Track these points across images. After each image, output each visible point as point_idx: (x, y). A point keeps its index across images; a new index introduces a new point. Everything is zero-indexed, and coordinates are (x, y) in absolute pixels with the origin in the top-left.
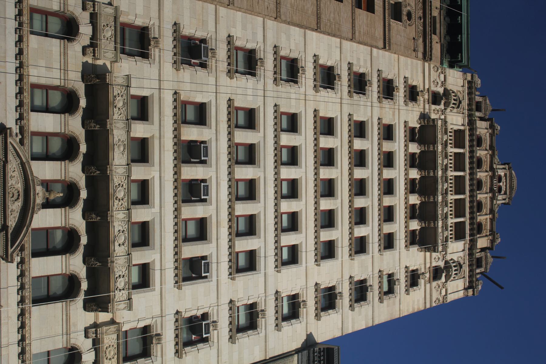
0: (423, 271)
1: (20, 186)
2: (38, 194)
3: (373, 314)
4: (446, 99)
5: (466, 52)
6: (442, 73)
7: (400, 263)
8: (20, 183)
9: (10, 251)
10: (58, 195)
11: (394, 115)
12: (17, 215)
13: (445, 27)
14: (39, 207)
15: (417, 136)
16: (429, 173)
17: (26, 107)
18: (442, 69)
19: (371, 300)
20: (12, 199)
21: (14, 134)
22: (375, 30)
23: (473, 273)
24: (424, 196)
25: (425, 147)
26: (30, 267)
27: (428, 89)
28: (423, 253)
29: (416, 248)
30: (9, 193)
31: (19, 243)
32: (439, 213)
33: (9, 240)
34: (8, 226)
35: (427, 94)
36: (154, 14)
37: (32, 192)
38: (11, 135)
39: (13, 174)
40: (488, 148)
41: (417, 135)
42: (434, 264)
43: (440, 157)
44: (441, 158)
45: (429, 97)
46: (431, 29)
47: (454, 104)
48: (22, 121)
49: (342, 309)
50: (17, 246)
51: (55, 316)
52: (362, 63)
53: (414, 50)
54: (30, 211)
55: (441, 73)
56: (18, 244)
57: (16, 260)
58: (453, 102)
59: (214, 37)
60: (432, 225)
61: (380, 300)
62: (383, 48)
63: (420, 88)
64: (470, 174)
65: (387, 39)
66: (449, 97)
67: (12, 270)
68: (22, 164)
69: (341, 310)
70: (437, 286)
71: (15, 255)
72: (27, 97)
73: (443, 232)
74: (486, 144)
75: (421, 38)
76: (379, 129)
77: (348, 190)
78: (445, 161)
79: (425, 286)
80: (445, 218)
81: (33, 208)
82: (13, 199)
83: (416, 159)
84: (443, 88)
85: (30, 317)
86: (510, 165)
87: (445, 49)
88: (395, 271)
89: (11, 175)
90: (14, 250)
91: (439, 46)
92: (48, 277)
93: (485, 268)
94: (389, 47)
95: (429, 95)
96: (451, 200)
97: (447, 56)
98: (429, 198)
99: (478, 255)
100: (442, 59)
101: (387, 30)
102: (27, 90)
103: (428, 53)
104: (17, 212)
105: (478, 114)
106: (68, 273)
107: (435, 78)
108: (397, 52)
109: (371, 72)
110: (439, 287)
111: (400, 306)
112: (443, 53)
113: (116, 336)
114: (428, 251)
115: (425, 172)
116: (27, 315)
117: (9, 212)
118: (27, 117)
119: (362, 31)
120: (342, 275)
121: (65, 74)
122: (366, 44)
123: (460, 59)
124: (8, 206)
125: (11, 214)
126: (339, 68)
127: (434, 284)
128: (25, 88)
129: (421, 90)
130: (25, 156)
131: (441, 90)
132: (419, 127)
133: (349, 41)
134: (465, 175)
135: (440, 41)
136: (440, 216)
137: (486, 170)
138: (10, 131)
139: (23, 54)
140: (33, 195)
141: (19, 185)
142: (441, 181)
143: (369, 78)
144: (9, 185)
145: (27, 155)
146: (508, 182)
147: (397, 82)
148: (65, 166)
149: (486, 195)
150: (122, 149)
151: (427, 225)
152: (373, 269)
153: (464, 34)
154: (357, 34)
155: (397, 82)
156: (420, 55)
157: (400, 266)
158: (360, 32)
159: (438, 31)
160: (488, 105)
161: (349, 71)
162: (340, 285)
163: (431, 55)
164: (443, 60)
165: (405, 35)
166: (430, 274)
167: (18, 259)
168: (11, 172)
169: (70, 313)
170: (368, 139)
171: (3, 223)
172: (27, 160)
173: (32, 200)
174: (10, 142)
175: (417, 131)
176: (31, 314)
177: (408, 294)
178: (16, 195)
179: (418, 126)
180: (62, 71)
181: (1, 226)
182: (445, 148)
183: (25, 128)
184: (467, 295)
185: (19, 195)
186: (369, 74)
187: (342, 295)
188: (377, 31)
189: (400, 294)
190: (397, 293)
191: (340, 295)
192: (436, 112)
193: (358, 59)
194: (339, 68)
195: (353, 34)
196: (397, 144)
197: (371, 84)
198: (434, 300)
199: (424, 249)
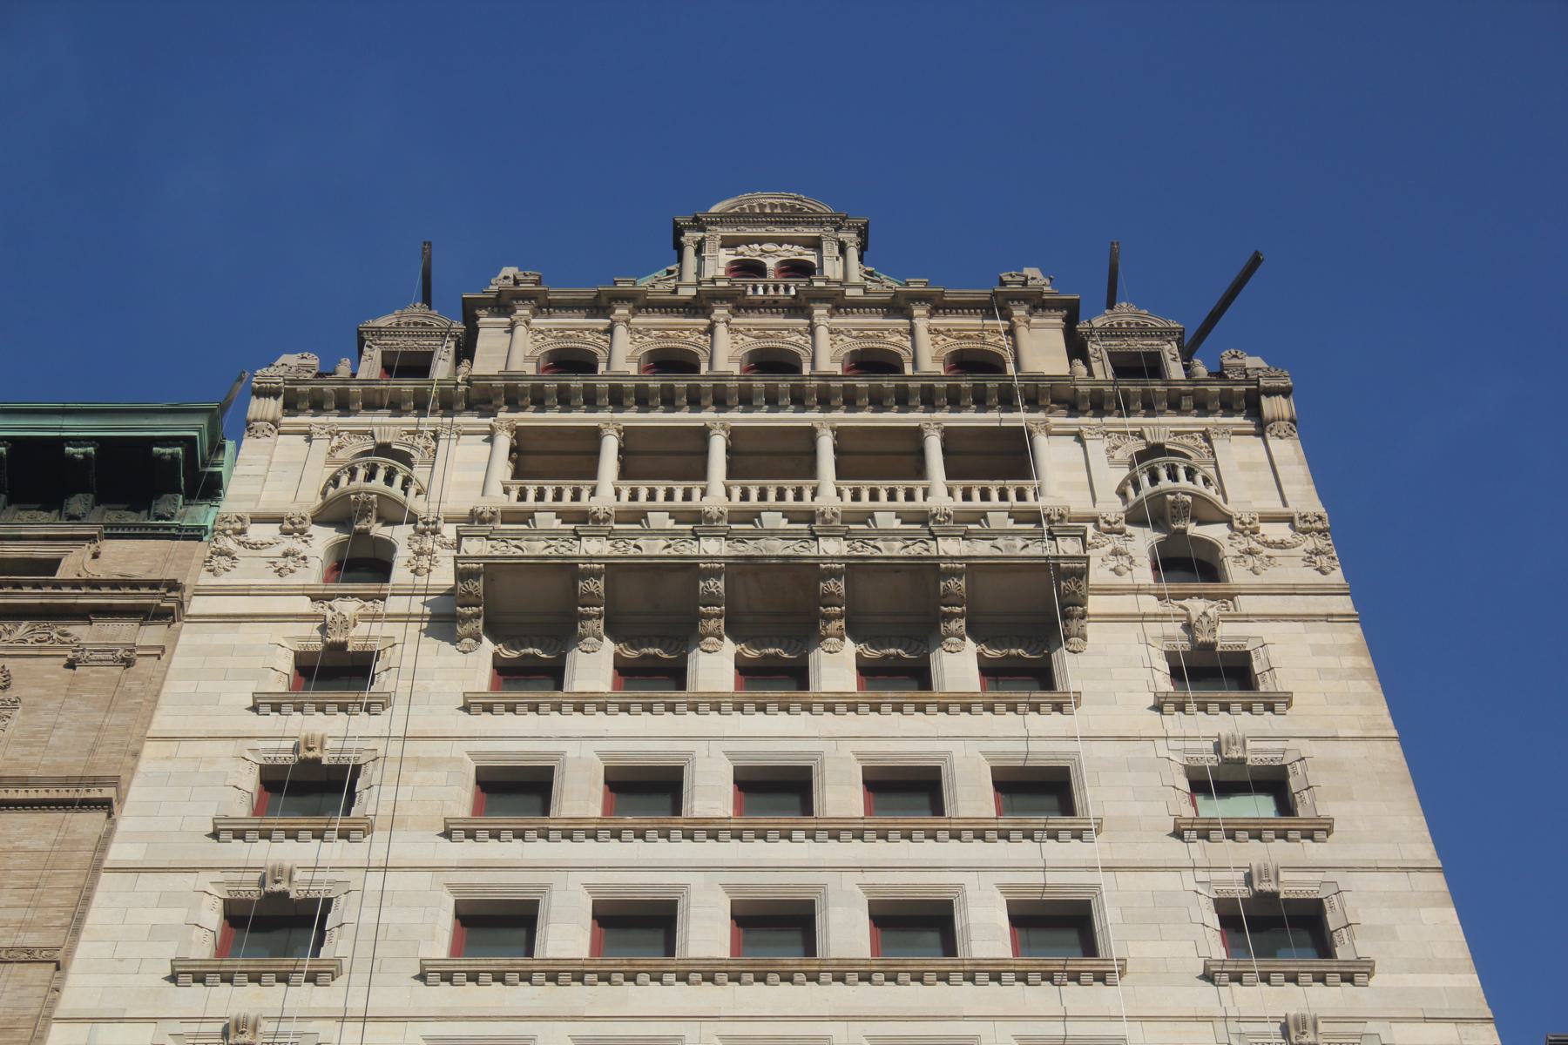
0: (1175, 629)
3: (1388, 869)
4: (364, 514)
5: (146, 422)
6: (242, 532)
7: (1140, 738)
11: (431, 763)
13: (25, 515)
15: (538, 652)
16: (712, 600)
18: (224, 531)
19: (1319, 876)
22: (16, 849)
23: (1186, 394)
24: (822, 623)
25: (589, 617)
27: (314, 598)
28: (1091, 629)
29: (1068, 657)
32: (903, 553)
35: (336, 603)
40: (602, 323)
41: (531, 650)
42: (1144, 574)
43: (636, 546)
44: (641, 542)
45: (353, 596)
46: (27, 584)
47: (389, 480)
49: (1363, 1020)
52: (176, 916)
53: (128, 663)
55: (242, 538)
58: (378, 483)
60: (957, 585)
61: (1318, 835)
62: (109, 815)
63: (309, 639)
64: (721, 404)
65: (63, 794)
66: (356, 503)
69: (1371, 1027)
70: (1250, 559)
73: (990, 536)
74: (582, 331)
75: (70, 629)
76: (495, 835)
77: (786, 986)
78: (660, 520)
79: (1247, 618)
80: (925, 523)
83: (645, 656)
84: (314, 530)
86: (683, 220)
87: (131, 518)
88: (1178, 759)
91: (111, 548)
93: (1160, 337)
94: (105, 785)
95: (344, 596)
96: (839, 493)
97: (161, 507)
98: (830, 599)
99: (1103, 371)
100: (173, 531)
101: (21, 795)
103: (145, 598)
105: (442, 368)
107: (263, 563)
108: (133, 747)
109: (223, 869)
110: (1250, 552)
111: (1346, 738)
112: (147, 527)
114: (1082, 603)
115: (709, 617)
119: (17, 915)
120: (1197, 1019)
122: (85, 898)
123: (179, 450)
126: (194, 1028)
127: (1237, 574)
129: (318, 634)
131: (324, 538)
132: (495, 640)
133: (63, 978)
134: (723, 428)
135: (91, 538)
136: (917, 549)
137: (705, 333)
142: (752, 543)
143: (248, 883)
146: (760, 232)
147: (274, 744)
149: (822, 334)
151: (958, 610)
152: (1166, 869)
153: (61, 429)
154: (31, 939)
155: (274, 744)
156: (152, 634)
157: (1152, 738)
158: (24, 926)
159: (42, 551)
160: (403, 320)
161: (209, 978)
162: (1245, 1027)
163: (154, 585)
164: (180, 528)
165: (52, 705)
166: (1191, 596)
170: (545, 888)
175: (514, 654)
177: (1287, 699)
179: (488, 647)
182: (597, 521)
184: (1292, 420)
186: (231, 883)
187: (1296, 1019)
188: (24, 843)
189: (1286, 738)
190: (1284, 751)
191: (1297, 1029)
192: (424, 561)
193: (156, 933)
194: (194, 1028)
195: (29, 957)
196: (571, 750)
197: (278, 873)
198: (1319, 578)
199: (1074, 625)
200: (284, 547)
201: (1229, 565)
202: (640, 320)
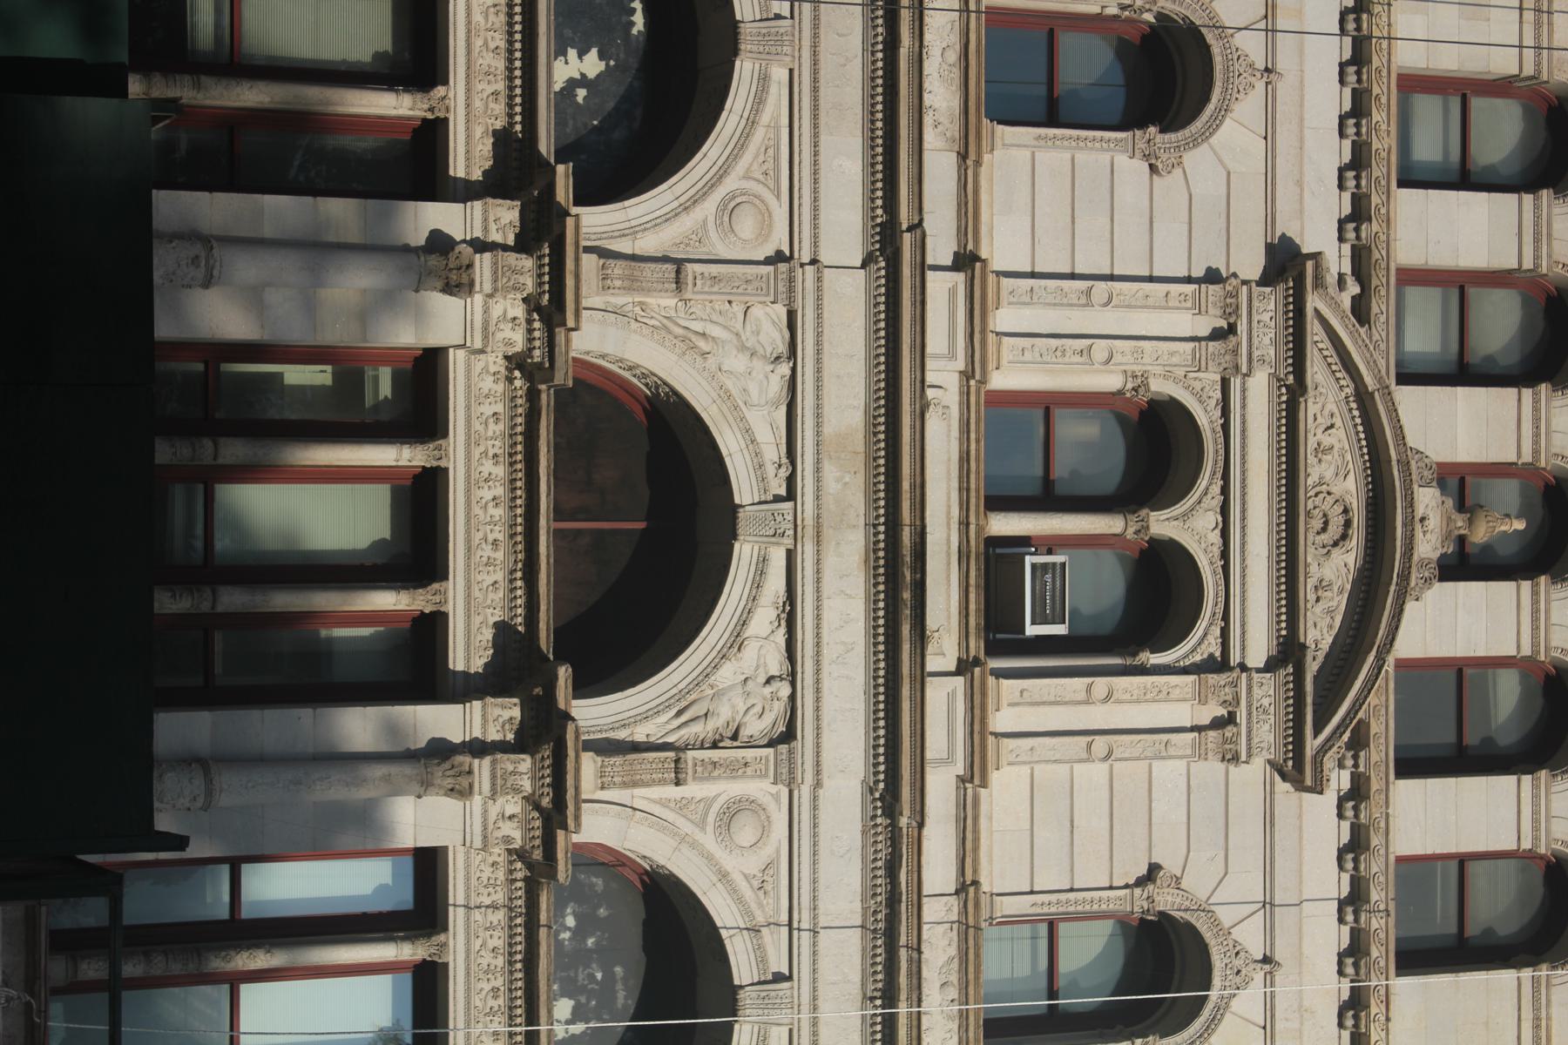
1: (1351, 488)
2: (1422, 519)
8: (1351, 477)
9: (1312, 744)
10: (1503, 528)
12: (1337, 602)
14: (1427, 574)
17: (1377, 171)
20: (1319, 539)
21: (1331, 279)
26: (1387, 814)
30: (1308, 513)
31: (1348, 713)
33: (1309, 700)
34: (1304, 647)
37: (1399, 511)
38: (1319, 282)
39: (1327, 440)
48: (1364, 227)
50: (1338, 727)
51: (1487, 1024)
54: (1393, 588)
56: (1343, 720)
57: (1333, 784)
68: (1363, 398)
71: (1329, 762)
72: (1384, 127)
81: (1405, 577)
85: (1388, 1019)
89: (1319, 444)
90: (1328, 740)
92: (1462, 861)
102: (1384, 100)
104: (1341, 592)
106: (1542, 850)
116: (1374, 1010)
117: (1307, 591)
118: (1383, 211)
121: (1538, 25)
124: (1307, 565)
125: (1318, 600)
128: (1376, 90)
130: (1372, 364)
138: (1317, 267)
140: (1404, 525)
141: (1350, 484)
144: (1310, 482)
145: (1382, 363)
148: (1536, 409)
167: (1340, 780)
168: (1319, 431)
169: (1548, 1018)
171: (1284, 633)
172: (1380, 380)
173: (1398, 543)
174: (1317, 311)
176: (1392, 1007)
178: (1337, 522)
180: (1529, 16)
181: (1278, 645)
183: (1376, 255)
185: (1348, 524)
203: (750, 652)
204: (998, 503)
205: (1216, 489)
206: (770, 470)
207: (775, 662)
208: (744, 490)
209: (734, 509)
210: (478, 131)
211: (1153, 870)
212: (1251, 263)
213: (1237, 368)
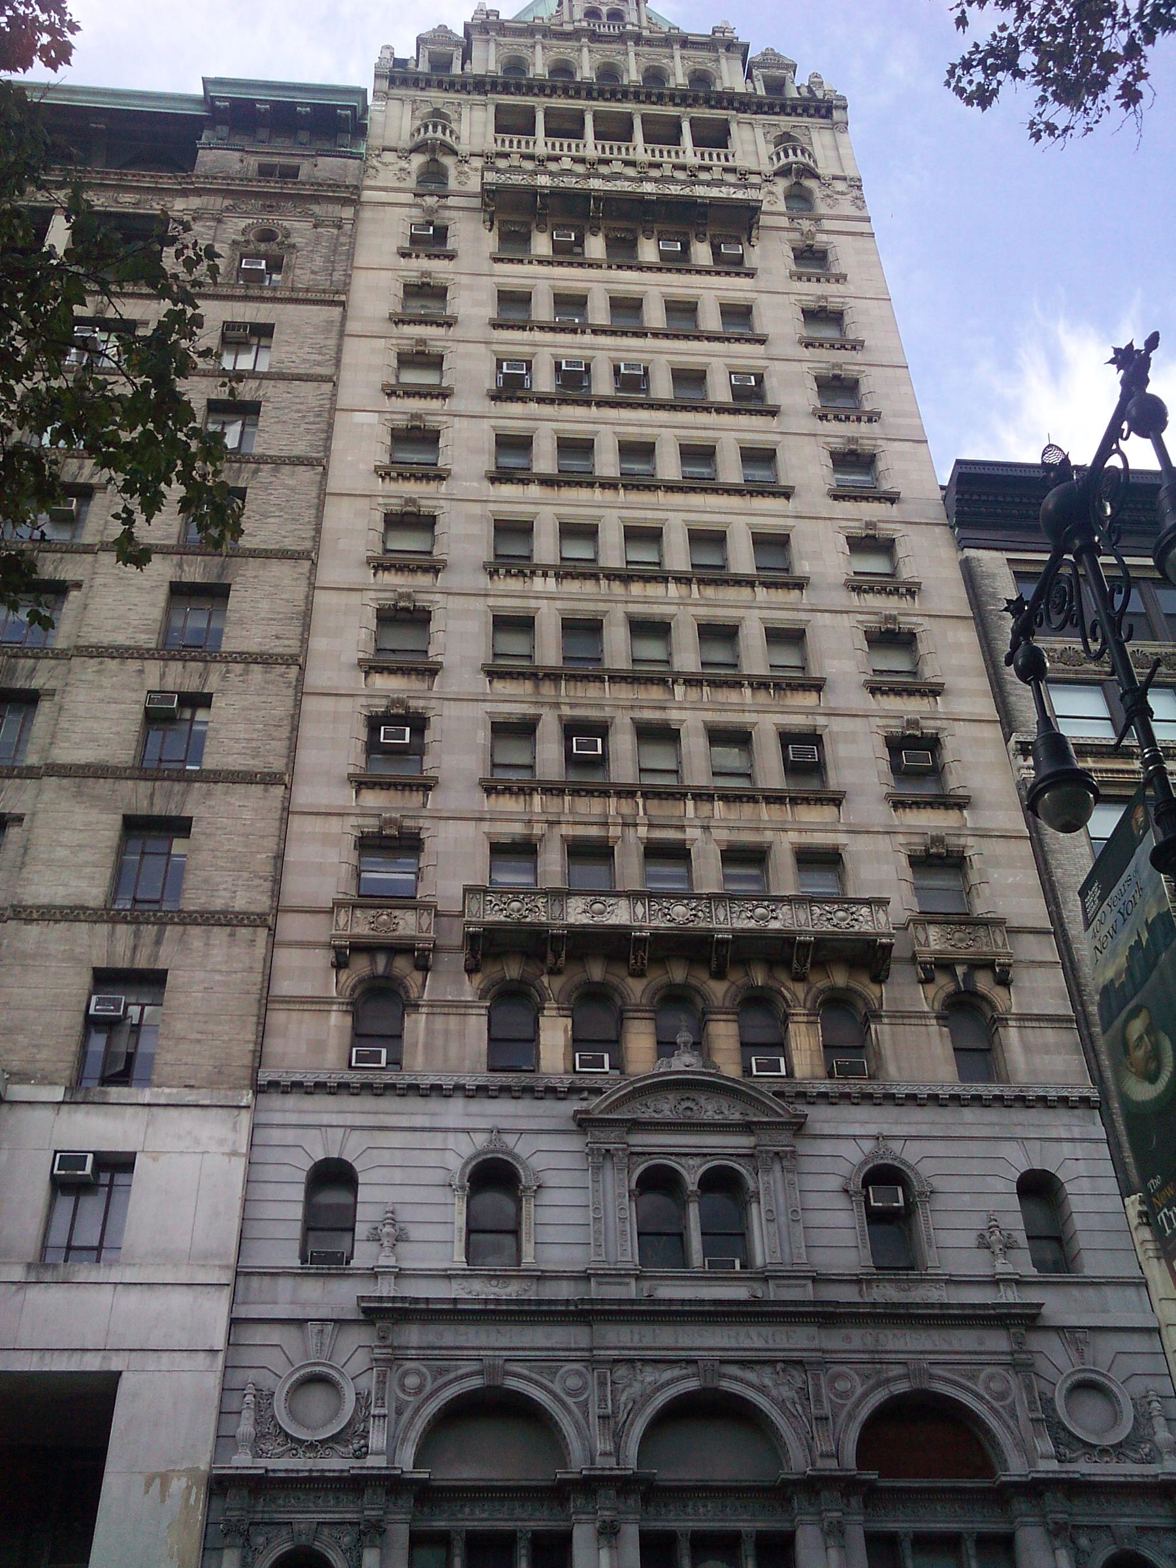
36: (334, 825)
38: (587, 1112)
40: (530, 41)
42: (781, 206)
49: (876, 439)
59: (363, 701)
64: (589, 97)
67: (820, 1117)
70: (829, 201)
82: (695, 1108)
93: (786, 69)
99: (761, 91)
105: (456, 69)
110: (829, 196)
113: (931, 927)
127: (822, 208)
136: (687, 191)
139: (441, 1086)
150: (597, 906)
177: (845, 277)
185: (688, 1099)
192: (463, 179)
200: (397, 167)
201: (818, 201)
202: (547, 42)
203: (767, 1382)
204: (685, 1262)
205: (678, 1160)
206: (684, 1372)
207: (768, 1370)
208: (692, 1385)
209: (704, 1390)
210: (538, 1514)
211: (846, 1191)
212: (575, 1143)
213: (624, 1150)
